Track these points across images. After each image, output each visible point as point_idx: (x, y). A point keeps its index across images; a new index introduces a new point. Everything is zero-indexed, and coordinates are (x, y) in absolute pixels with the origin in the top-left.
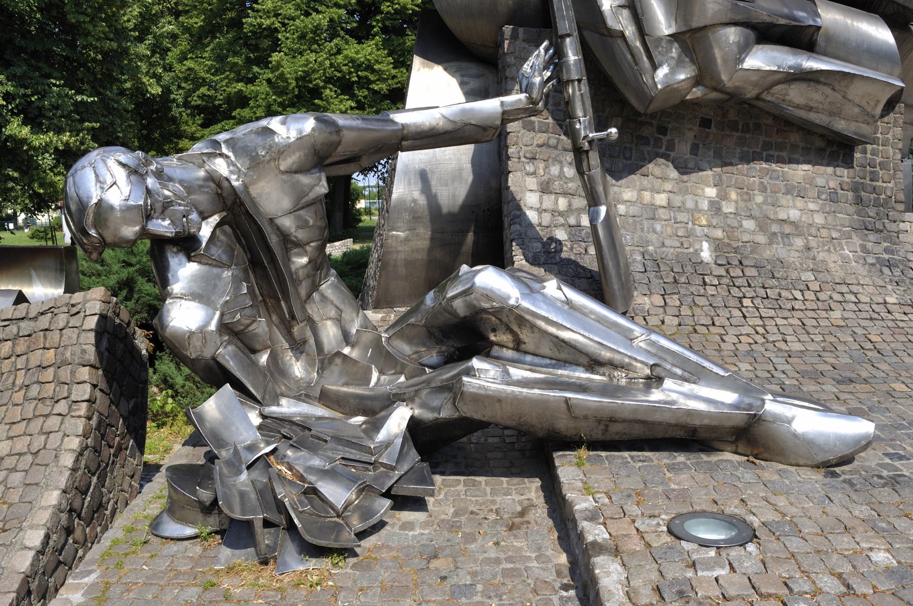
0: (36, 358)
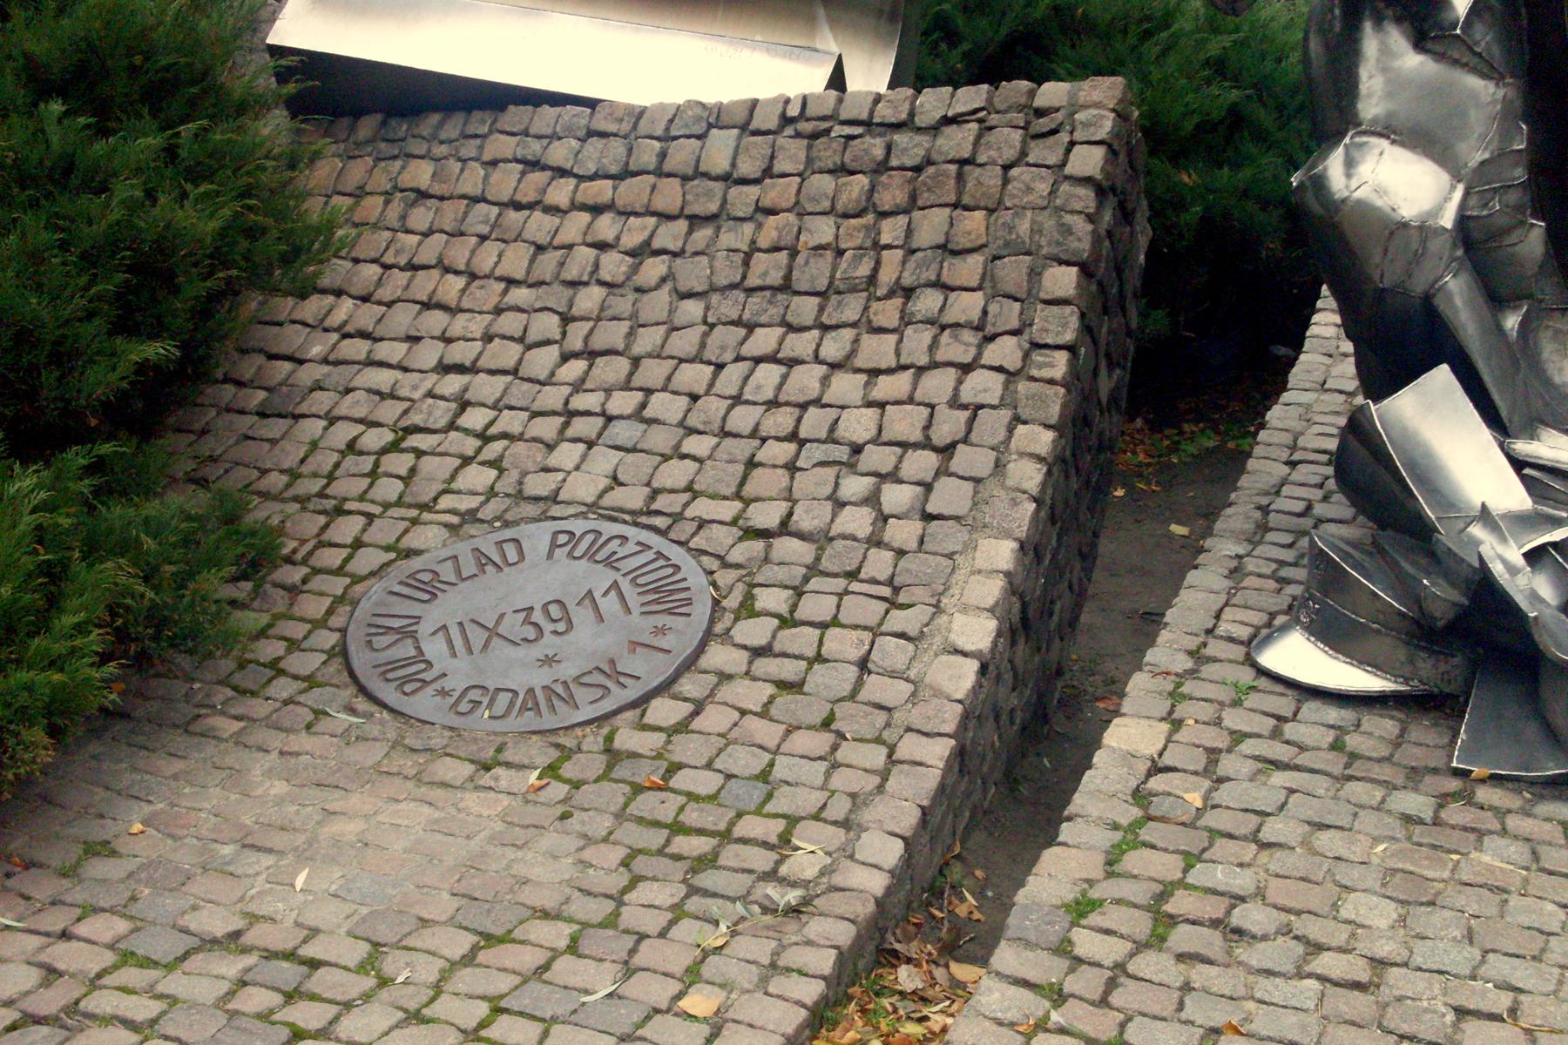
0: (931, 226)
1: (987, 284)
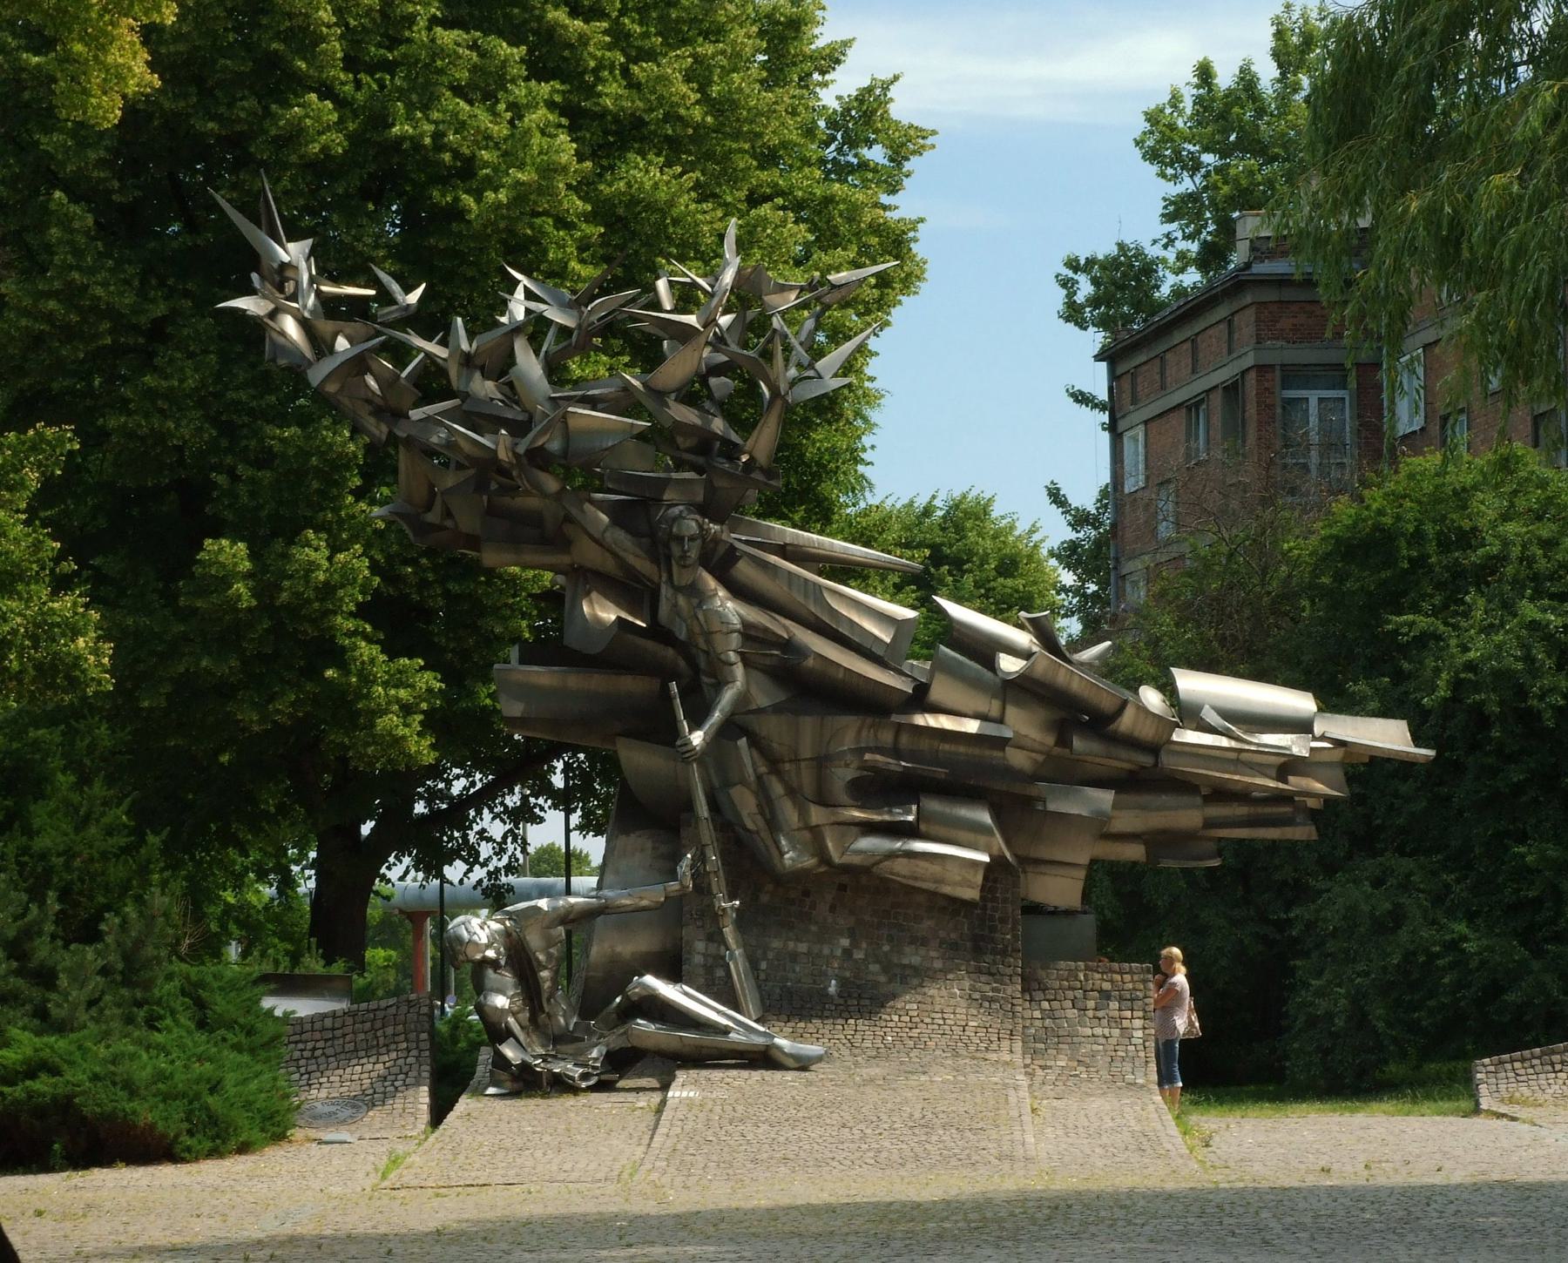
0: (390, 1030)
1: (407, 1040)
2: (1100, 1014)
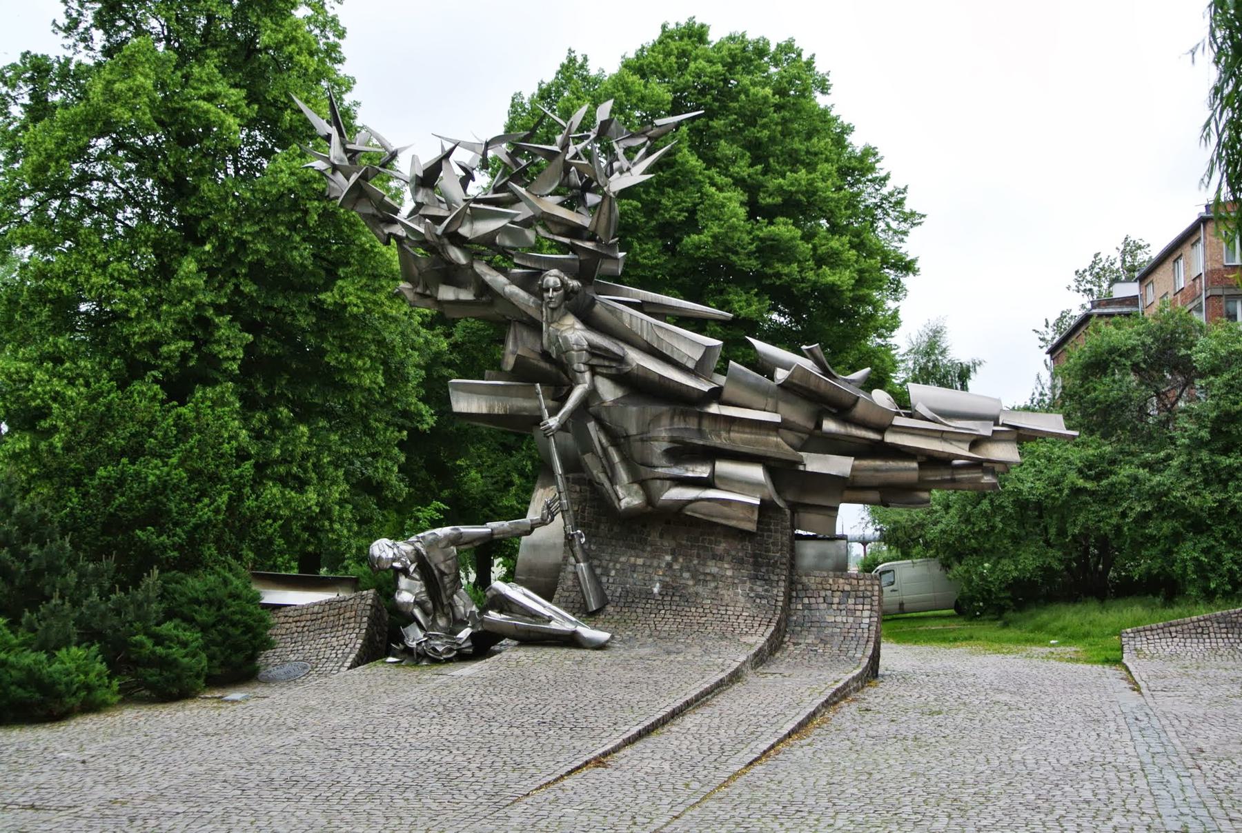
0: (347, 615)
2: (842, 607)
